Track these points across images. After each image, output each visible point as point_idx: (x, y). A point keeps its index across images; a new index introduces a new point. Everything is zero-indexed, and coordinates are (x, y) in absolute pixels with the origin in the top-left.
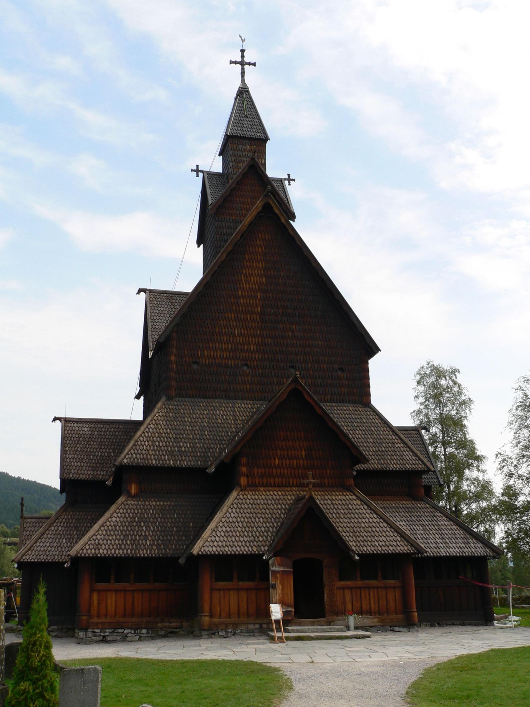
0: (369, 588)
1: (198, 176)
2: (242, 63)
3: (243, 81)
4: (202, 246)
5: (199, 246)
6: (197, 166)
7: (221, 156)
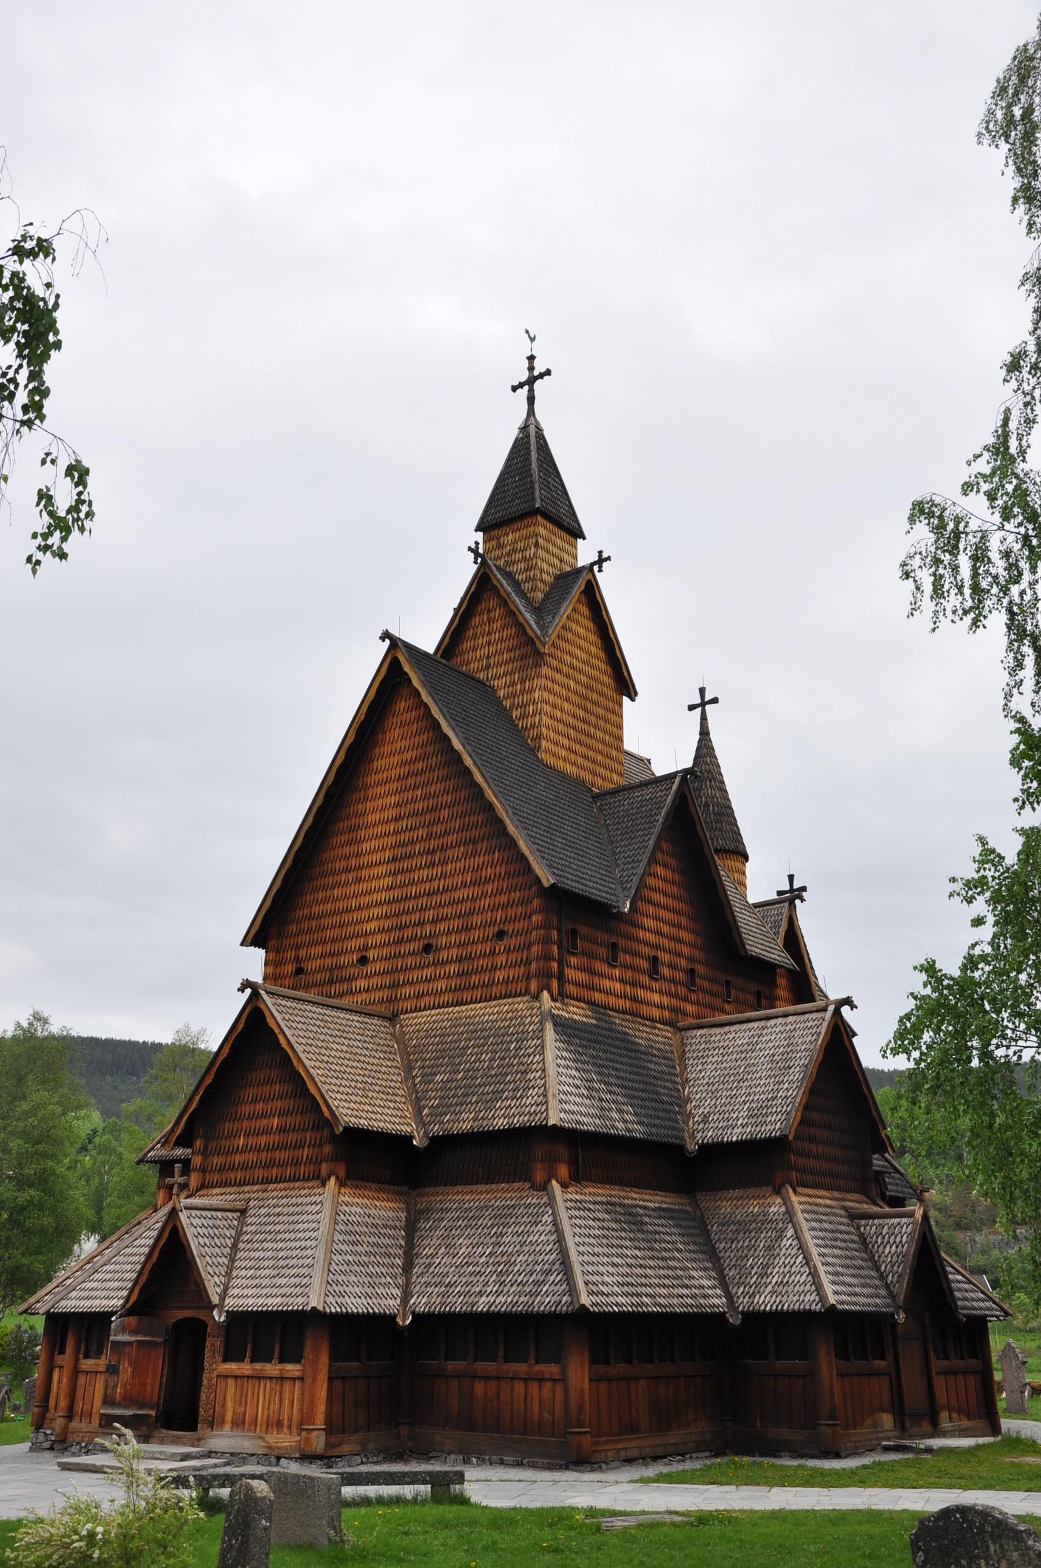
1: (475, 562)
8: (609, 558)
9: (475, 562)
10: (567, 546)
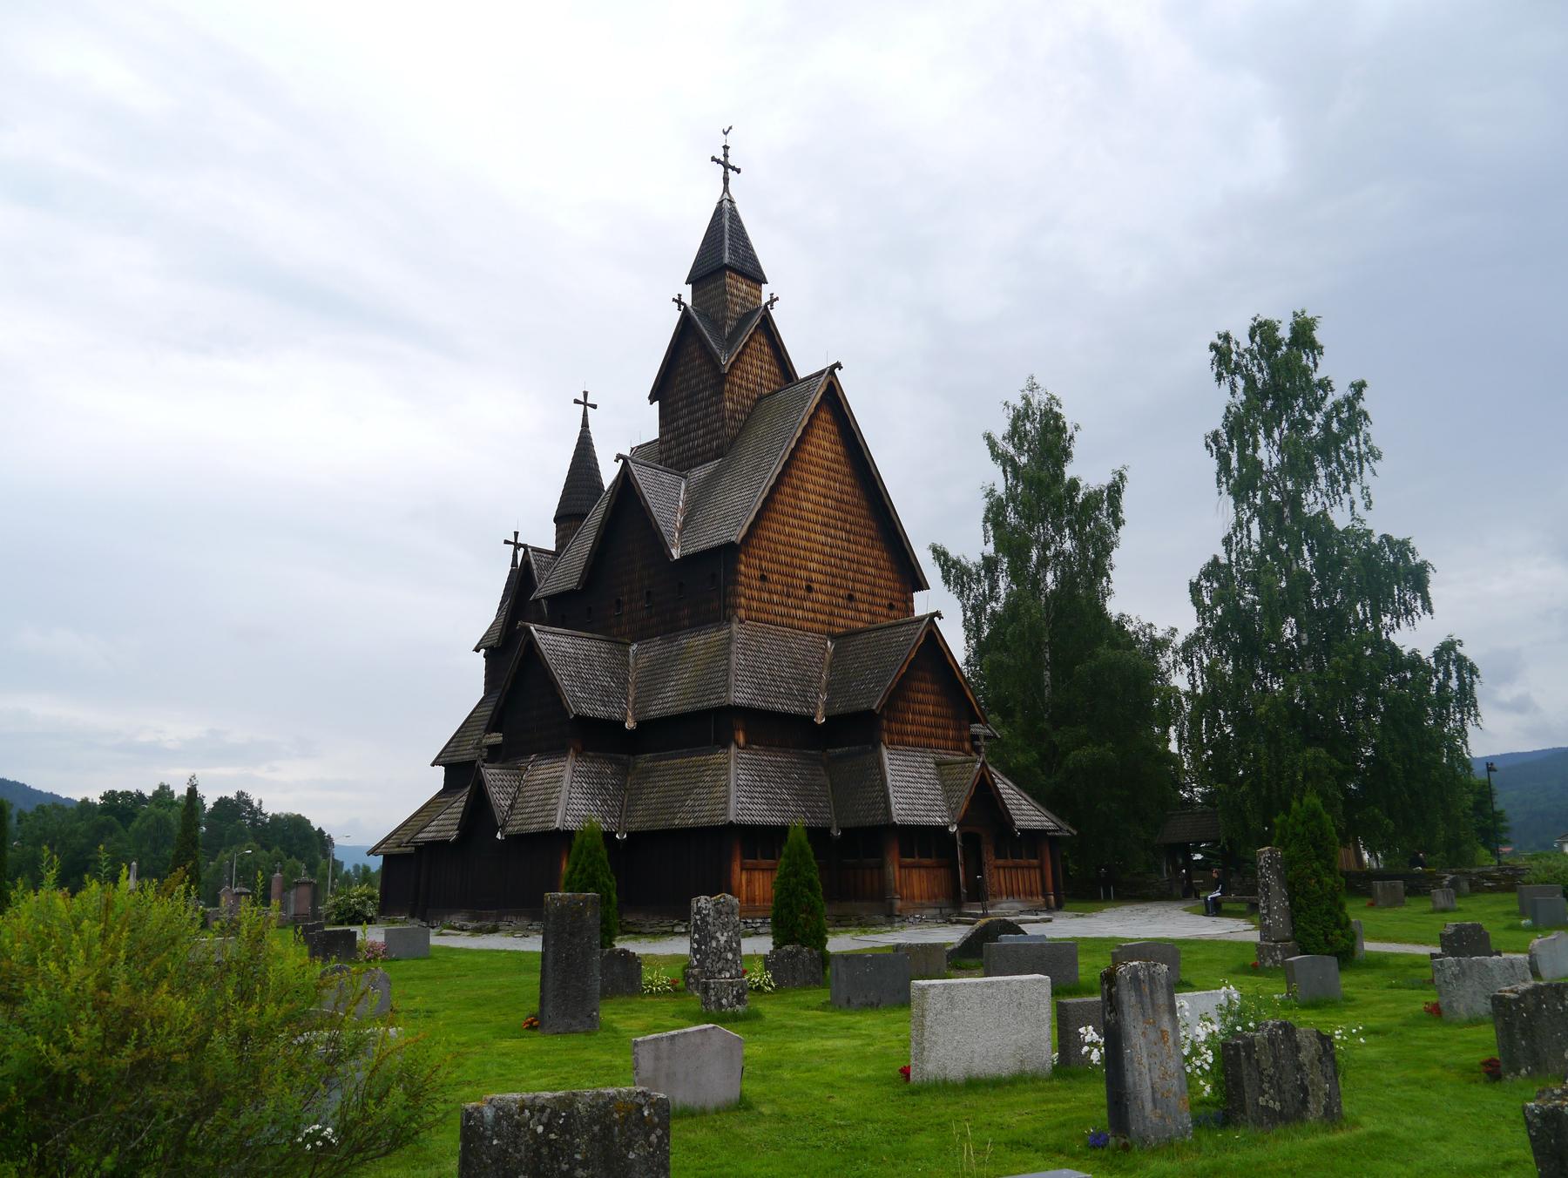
0: (1017, 867)
1: (679, 310)
2: (726, 166)
3: (726, 189)
5: (651, 404)
6: (680, 295)
8: (777, 299)
9: (679, 310)
10: (754, 291)
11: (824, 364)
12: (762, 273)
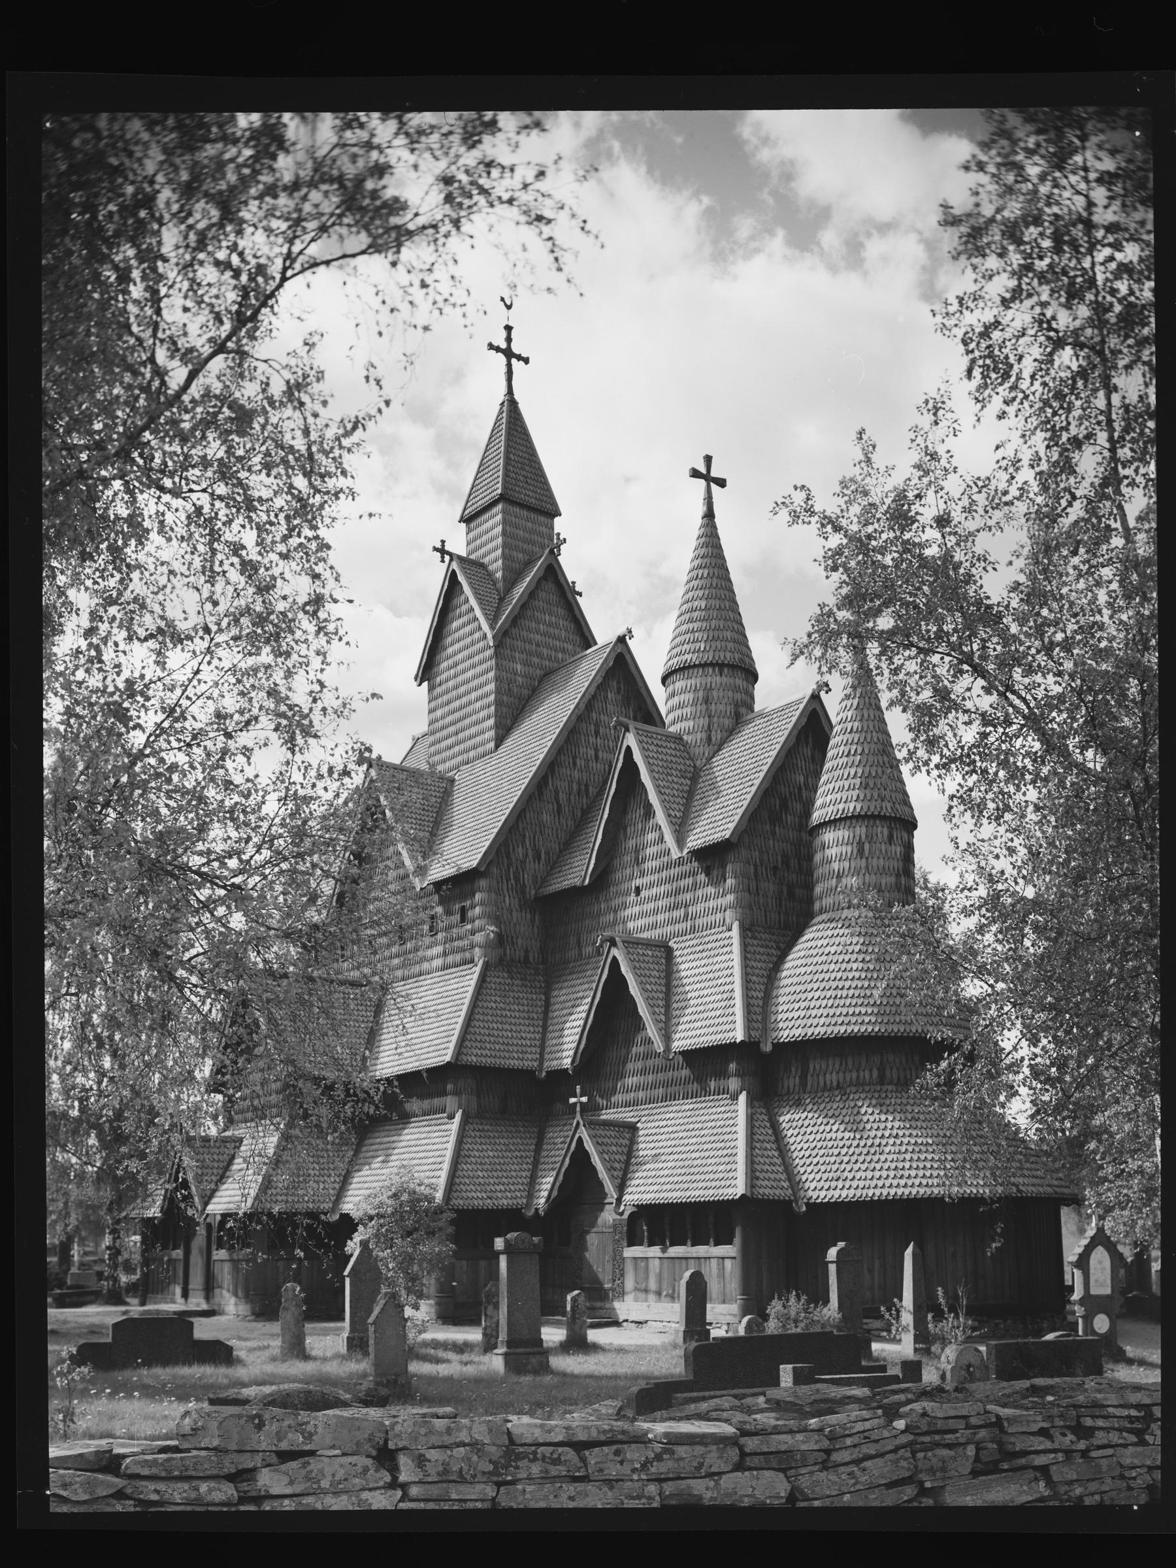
2: (509, 354)
4: (425, 684)
6: (443, 542)
7: (463, 525)
11: (621, 631)
12: (554, 503)
